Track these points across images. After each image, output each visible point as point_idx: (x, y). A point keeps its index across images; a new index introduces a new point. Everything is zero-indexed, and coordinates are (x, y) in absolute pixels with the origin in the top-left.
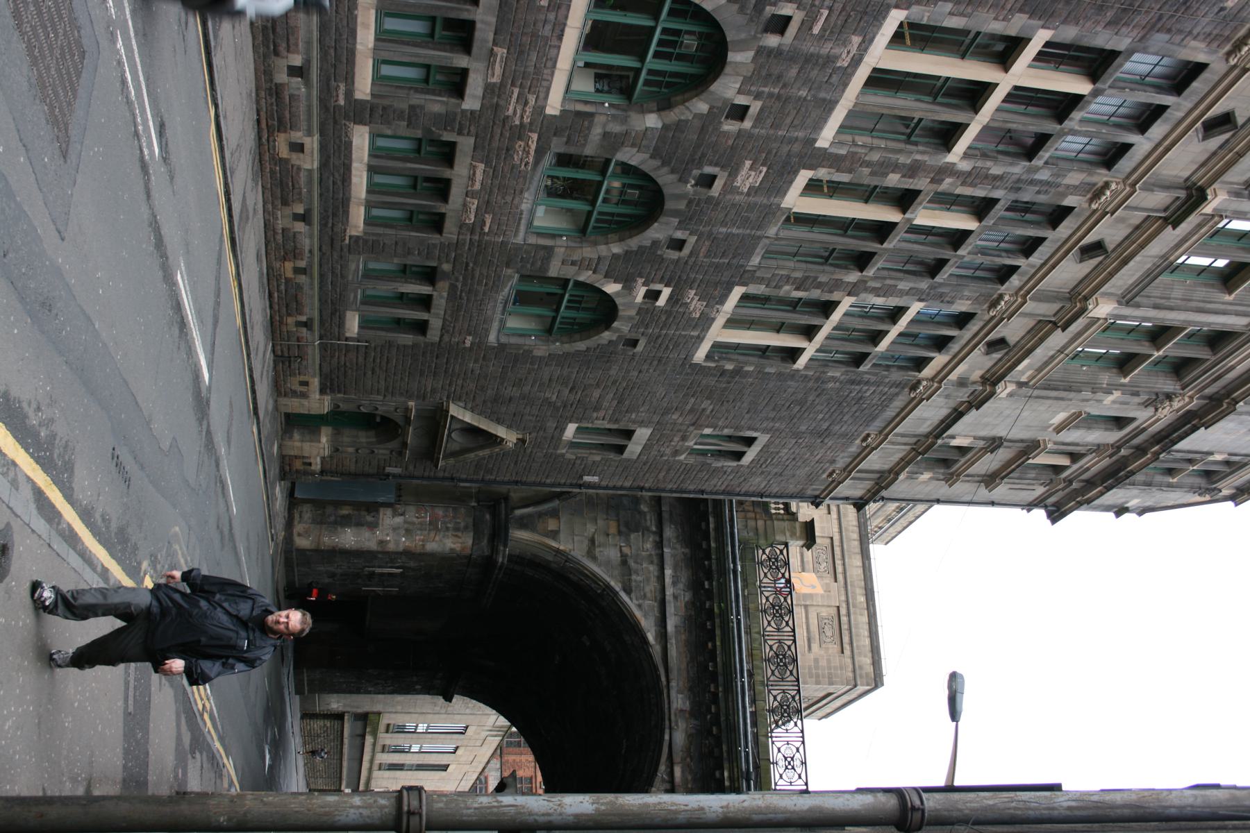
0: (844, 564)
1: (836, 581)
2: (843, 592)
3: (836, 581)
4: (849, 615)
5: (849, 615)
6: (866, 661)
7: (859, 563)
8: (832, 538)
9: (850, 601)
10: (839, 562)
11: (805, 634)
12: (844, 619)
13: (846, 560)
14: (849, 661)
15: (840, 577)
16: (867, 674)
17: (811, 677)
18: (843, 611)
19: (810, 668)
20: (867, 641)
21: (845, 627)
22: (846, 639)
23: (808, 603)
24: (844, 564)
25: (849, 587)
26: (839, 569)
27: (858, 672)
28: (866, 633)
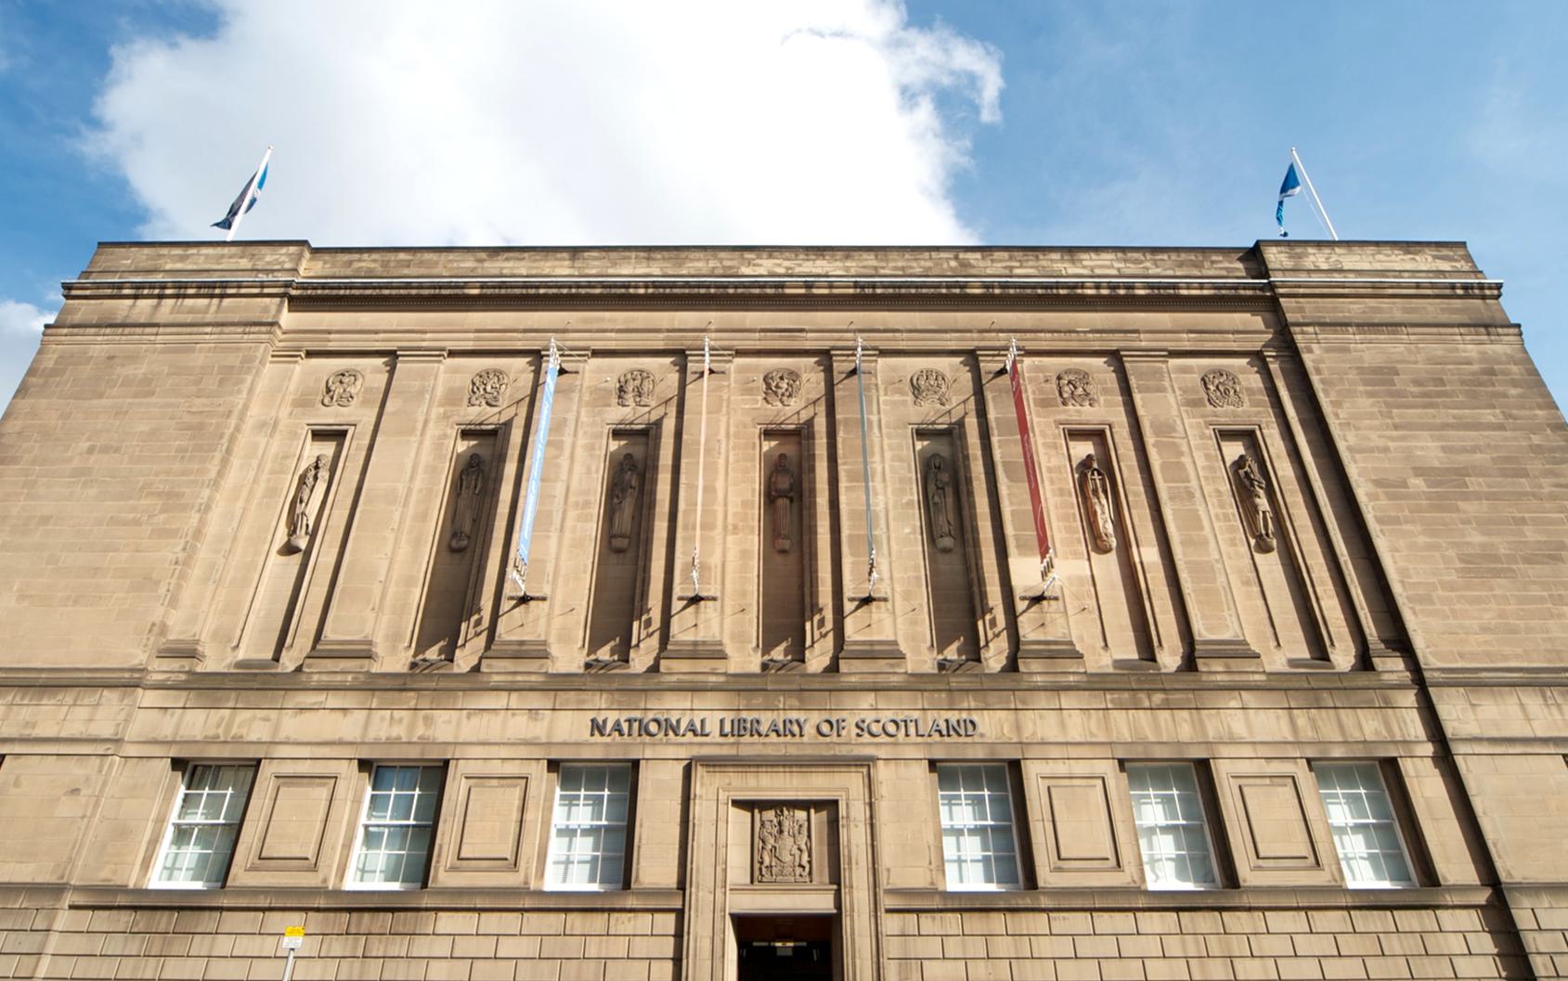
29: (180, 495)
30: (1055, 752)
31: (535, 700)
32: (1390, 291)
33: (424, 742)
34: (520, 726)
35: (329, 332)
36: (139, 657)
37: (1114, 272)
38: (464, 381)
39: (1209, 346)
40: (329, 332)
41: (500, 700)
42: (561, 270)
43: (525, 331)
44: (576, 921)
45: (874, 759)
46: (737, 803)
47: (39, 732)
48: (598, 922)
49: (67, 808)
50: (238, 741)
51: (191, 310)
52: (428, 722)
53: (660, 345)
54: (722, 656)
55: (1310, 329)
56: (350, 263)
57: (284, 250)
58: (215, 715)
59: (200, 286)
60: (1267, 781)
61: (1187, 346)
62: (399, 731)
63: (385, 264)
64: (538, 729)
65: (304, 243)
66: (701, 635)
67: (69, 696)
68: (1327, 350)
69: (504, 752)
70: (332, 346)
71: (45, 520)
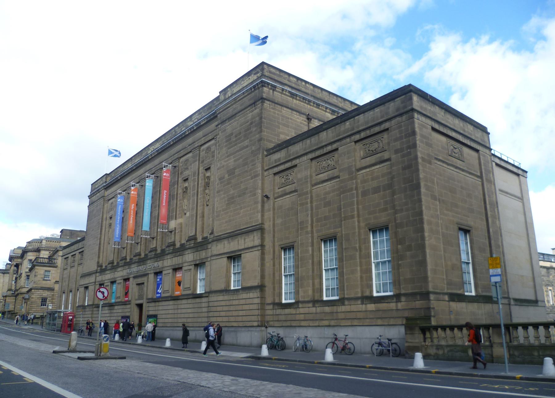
0: (326, 146)
1: (337, 149)
2: (344, 141)
3: (337, 149)
4: (359, 132)
5: (359, 132)
6: (392, 107)
7: (324, 133)
8: (312, 159)
9: (349, 133)
10: (325, 150)
11: (378, 166)
12: (363, 135)
13: (324, 144)
14: (393, 122)
15: (335, 146)
16: (402, 102)
17: (409, 153)
18: (357, 137)
19: (403, 156)
20: (377, 110)
21: (368, 133)
22: (377, 129)
23: (354, 169)
24: (326, 146)
25: (341, 137)
26: (329, 148)
27: (402, 111)
28: (371, 113)
30: (166, 269)
32: (238, 99)
35: (109, 195)
37: (197, 120)
39: (206, 140)
40: (109, 195)
42: (130, 165)
43: (125, 185)
45: (148, 274)
46: (137, 284)
55: (219, 126)
60: (188, 271)
61: (203, 142)
63: (114, 174)
65: (106, 174)
68: (222, 132)
70: (110, 198)
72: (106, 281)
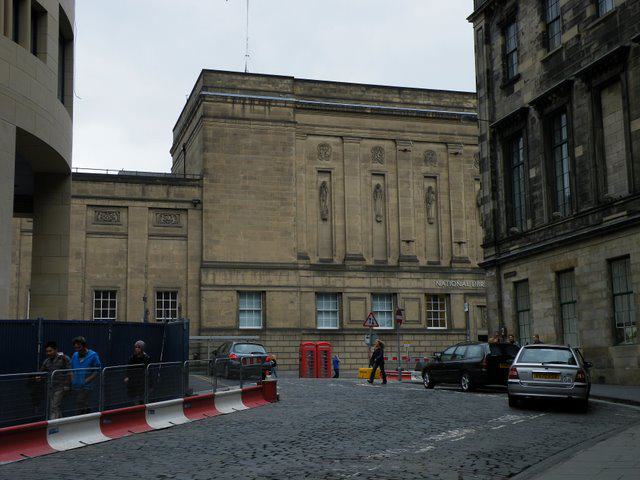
29: (285, 199)
31: (418, 276)
33: (389, 288)
34: (415, 283)
36: (295, 260)
38: (367, 151)
41: (407, 275)
44: (439, 337)
47: (273, 284)
48: (444, 337)
49: (291, 307)
50: (335, 287)
51: (259, 112)
52: (389, 281)
53: (438, 140)
54: (468, 262)
56: (311, 88)
57: (285, 81)
58: (324, 279)
59: (260, 100)
62: (380, 284)
64: (420, 284)
66: (462, 255)
67: (279, 272)
69: (413, 291)
71: (241, 207)
72: (348, 290)
